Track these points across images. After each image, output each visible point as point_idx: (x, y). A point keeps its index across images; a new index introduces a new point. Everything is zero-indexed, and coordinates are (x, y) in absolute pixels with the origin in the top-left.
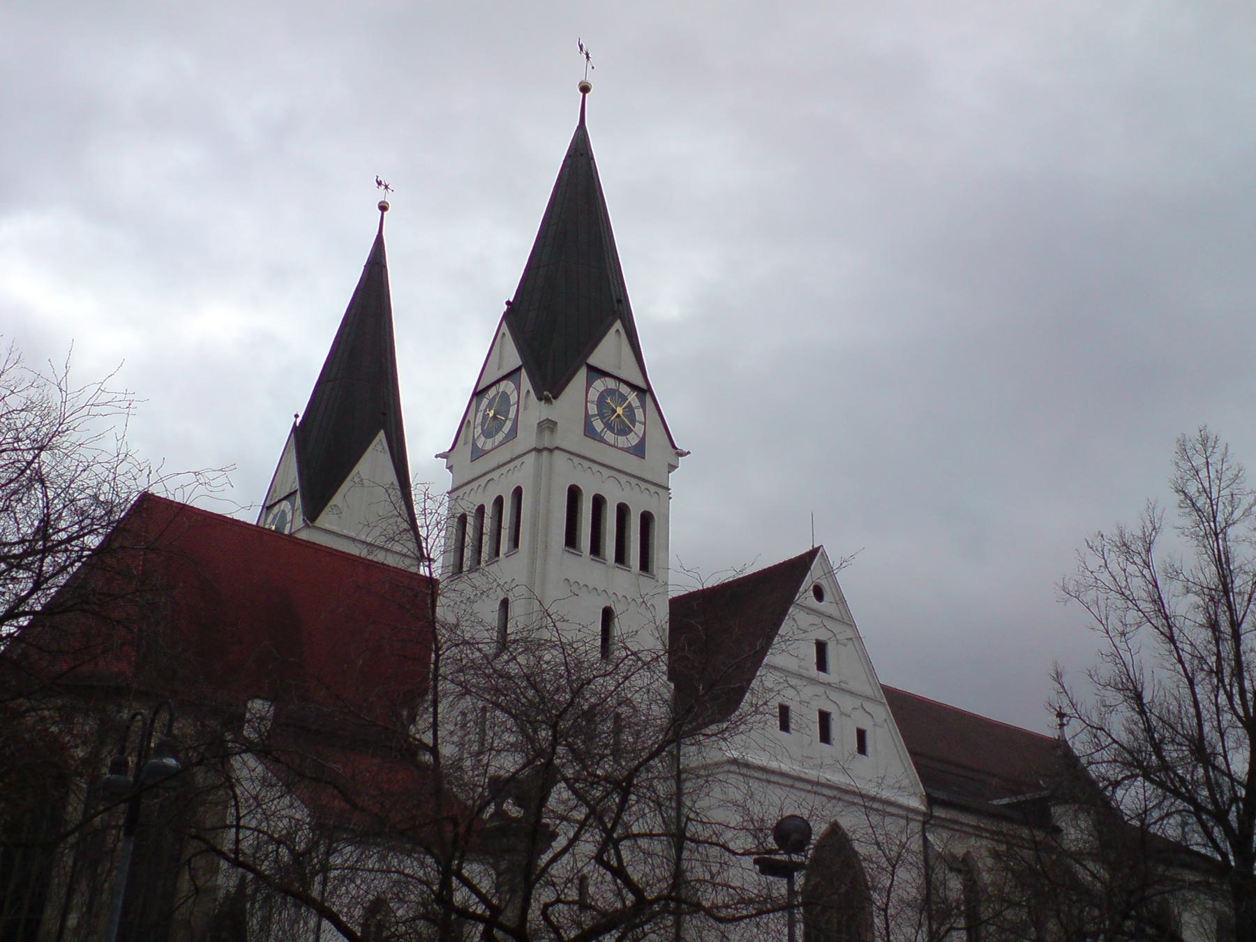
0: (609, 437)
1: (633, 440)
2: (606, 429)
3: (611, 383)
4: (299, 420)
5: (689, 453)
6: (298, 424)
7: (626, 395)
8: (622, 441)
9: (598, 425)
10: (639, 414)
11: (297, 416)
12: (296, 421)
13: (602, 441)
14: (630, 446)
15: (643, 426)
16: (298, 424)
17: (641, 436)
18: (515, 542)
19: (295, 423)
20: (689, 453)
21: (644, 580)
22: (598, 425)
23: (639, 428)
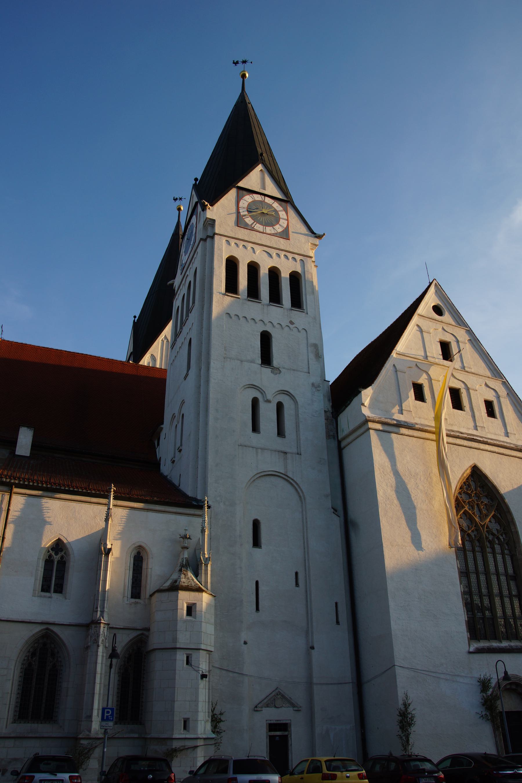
0: (258, 227)
1: (279, 229)
2: (255, 223)
3: (258, 197)
4: (136, 319)
5: (324, 234)
6: (136, 321)
7: (271, 204)
8: (269, 230)
9: (249, 220)
10: (282, 214)
11: (135, 317)
12: (135, 319)
13: (253, 229)
14: (276, 232)
15: (287, 221)
16: (136, 321)
17: (285, 227)
18: (194, 302)
19: (134, 321)
20: (324, 234)
21: (296, 315)
22: (249, 220)
23: (283, 223)
